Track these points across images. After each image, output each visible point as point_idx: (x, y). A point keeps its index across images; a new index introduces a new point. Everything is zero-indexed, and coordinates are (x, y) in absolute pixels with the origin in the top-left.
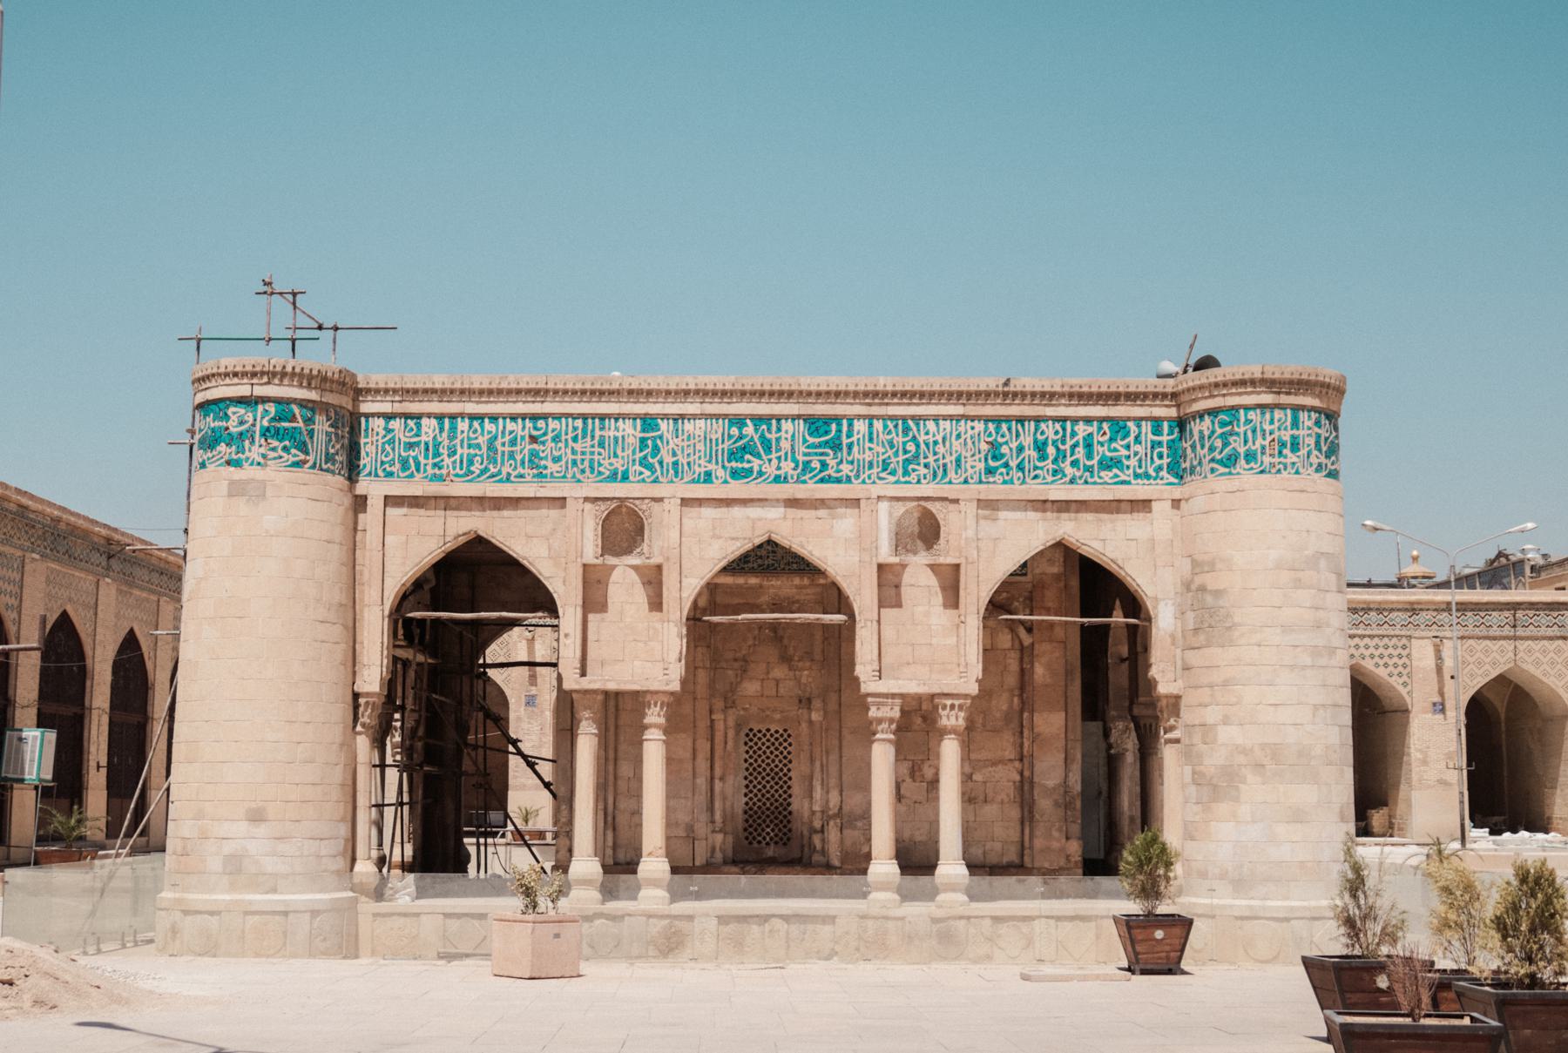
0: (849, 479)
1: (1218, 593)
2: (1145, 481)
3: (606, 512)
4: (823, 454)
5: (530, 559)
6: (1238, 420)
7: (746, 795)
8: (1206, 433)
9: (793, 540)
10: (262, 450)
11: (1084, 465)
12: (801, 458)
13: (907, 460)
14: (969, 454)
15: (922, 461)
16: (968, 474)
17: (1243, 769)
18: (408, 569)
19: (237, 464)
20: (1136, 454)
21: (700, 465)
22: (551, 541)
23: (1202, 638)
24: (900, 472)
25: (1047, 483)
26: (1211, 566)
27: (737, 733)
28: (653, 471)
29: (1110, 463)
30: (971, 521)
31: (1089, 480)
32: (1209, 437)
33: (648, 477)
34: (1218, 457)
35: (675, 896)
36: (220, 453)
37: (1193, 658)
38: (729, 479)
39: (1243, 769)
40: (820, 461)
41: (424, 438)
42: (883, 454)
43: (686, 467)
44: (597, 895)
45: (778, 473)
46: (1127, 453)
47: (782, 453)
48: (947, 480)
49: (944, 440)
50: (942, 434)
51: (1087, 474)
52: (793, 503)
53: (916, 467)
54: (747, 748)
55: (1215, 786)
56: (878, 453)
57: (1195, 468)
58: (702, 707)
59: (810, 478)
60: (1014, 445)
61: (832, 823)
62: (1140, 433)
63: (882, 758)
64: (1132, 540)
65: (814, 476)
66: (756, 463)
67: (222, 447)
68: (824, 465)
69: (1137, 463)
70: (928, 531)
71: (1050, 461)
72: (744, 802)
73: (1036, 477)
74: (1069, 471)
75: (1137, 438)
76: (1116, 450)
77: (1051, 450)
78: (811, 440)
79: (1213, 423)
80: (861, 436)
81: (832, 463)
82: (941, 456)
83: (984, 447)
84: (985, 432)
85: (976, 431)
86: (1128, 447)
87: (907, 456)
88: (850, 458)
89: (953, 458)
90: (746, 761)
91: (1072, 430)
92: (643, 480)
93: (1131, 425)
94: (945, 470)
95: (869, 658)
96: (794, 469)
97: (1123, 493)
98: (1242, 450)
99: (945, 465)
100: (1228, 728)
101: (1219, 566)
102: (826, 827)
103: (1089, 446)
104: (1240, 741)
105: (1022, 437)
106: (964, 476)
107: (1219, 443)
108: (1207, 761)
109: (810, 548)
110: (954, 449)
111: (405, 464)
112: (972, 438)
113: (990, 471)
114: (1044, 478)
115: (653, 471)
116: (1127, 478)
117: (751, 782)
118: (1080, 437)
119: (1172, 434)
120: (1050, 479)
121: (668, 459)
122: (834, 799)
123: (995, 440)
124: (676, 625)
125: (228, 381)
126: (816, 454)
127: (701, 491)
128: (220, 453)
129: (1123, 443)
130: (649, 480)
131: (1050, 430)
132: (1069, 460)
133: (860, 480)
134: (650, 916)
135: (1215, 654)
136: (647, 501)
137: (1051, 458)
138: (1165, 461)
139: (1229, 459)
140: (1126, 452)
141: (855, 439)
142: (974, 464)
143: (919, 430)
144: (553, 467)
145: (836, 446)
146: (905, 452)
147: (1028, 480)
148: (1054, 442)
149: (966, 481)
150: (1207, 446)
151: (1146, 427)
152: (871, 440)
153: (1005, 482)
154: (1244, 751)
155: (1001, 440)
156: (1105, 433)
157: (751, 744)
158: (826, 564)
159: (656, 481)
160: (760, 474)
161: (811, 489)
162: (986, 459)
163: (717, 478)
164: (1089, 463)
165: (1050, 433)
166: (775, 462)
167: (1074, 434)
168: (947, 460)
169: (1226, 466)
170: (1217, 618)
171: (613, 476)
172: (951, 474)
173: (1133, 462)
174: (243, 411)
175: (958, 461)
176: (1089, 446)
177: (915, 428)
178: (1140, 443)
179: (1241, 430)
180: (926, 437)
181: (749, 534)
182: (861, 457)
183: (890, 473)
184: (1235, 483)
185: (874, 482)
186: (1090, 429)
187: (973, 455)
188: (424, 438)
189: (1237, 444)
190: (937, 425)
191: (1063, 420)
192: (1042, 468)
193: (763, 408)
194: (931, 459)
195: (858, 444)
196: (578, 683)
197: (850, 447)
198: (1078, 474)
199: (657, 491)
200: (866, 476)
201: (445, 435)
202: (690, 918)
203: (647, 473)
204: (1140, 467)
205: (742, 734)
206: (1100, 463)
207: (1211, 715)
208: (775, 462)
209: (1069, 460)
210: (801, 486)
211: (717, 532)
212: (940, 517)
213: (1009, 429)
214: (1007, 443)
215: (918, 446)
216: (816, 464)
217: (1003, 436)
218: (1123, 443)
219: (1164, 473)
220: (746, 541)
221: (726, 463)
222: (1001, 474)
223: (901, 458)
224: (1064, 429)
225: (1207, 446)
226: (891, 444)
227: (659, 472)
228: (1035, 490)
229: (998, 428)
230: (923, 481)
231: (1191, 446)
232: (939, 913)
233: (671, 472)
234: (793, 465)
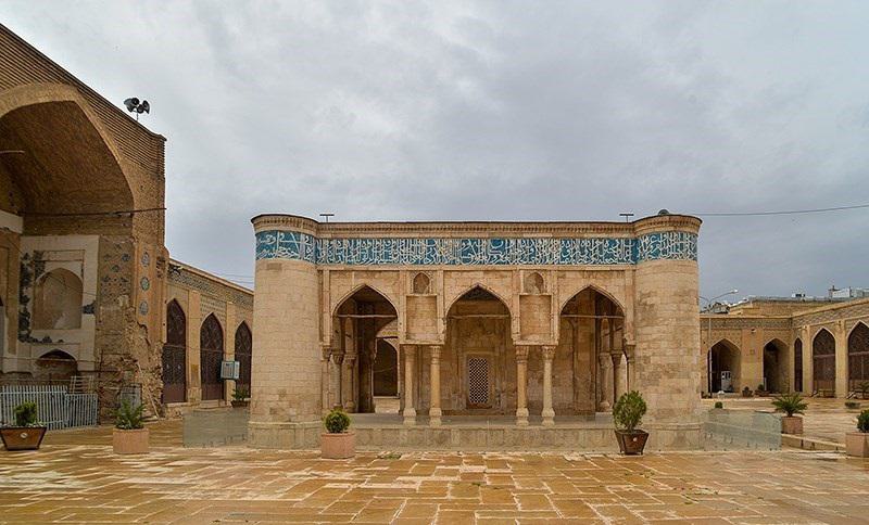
19: (271, 257)
30: (556, 279)
35: (444, 421)
44: (414, 422)
52: (486, 271)
58: (454, 351)
63: (521, 369)
68: (499, 258)
70: (539, 281)
74: (593, 259)
77: (586, 251)
97: (614, 267)
103: (601, 250)
113: (563, 259)
154: (660, 366)
171: (417, 263)
184: (658, 263)
193: (475, 235)
228: (580, 266)
232: (542, 428)
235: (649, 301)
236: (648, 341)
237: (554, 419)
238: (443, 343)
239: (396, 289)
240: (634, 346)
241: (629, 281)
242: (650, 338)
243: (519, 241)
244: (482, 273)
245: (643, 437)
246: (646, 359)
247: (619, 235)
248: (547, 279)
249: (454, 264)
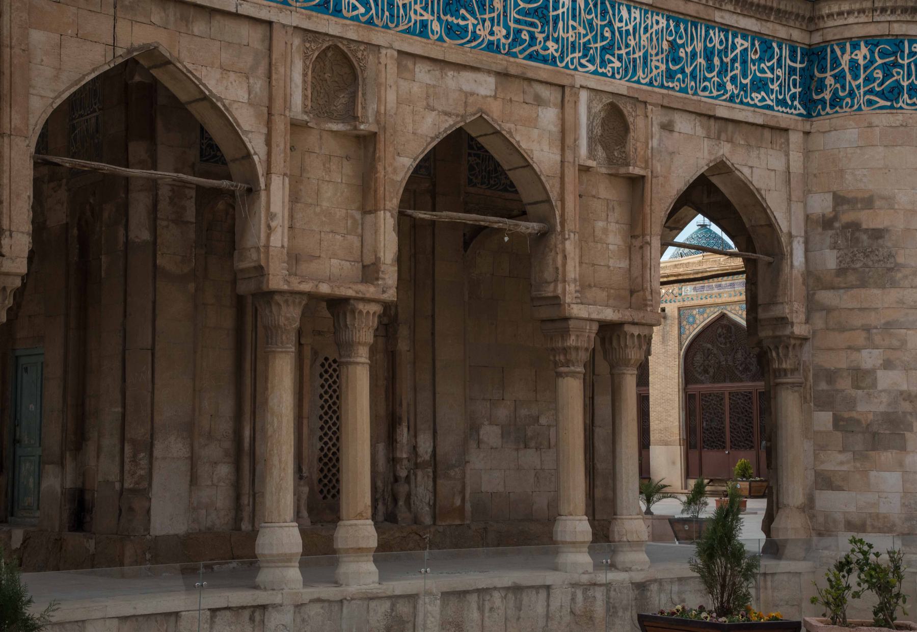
0: (554, 61)
1: (878, 234)
2: (784, 109)
3: (316, 54)
4: (532, 25)
5: (227, 102)
6: (903, 52)
7: (321, 439)
8: (862, 62)
9: (503, 125)
11: (741, 82)
12: (512, 25)
13: (603, 48)
14: (654, 52)
15: (617, 52)
16: (653, 75)
17: (909, 417)
18: (63, 87)
20: (778, 78)
21: (415, 12)
22: (251, 81)
23: (852, 278)
24: (598, 61)
25: (712, 97)
26: (868, 202)
27: (314, 361)
29: (760, 85)
30: (656, 129)
31: (745, 101)
32: (866, 68)
33: (363, 15)
34: (878, 89)
37: (826, 297)
38: (446, 39)
39: (909, 417)
40: (529, 32)
42: (585, 36)
43: (401, 11)
45: (491, 38)
46: (771, 76)
47: (495, 15)
48: (636, 78)
49: (634, 29)
50: (633, 24)
51: (742, 93)
53: (611, 58)
54: (322, 381)
55: (874, 435)
56: (579, 33)
57: (842, 99)
59: (522, 51)
60: (689, 50)
61: (420, 473)
62: (781, 56)
64: (772, 170)
65: (524, 50)
66: (471, 21)
68: (533, 37)
69: (778, 88)
71: (715, 73)
72: (319, 447)
73: (705, 89)
74: (729, 86)
75: (779, 60)
76: (763, 71)
77: (716, 61)
78: (522, 5)
79: (872, 52)
80: (565, 10)
81: (540, 37)
82: (631, 49)
83: (665, 45)
84: (667, 29)
85: (660, 26)
86: (772, 69)
87: (604, 43)
88: (556, 35)
89: (641, 54)
90: (321, 396)
91: (733, 42)
92: (355, 19)
93: (774, 45)
94: (635, 66)
95: (573, 277)
96: (507, 37)
98: (905, 84)
99: (635, 60)
100: (891, 373)
101: (878, 203)
102: (413, 477)
103: (744, 62)
104: (904, 387)
105: (695, 42)
106: (649, 76)
107: (879, 74)
108: (862, 407)
109: (518, 138)
110: (642, 43)
112: (657, 33)
113: (670, 75)
114: (711, 92)
115: (369, 9)
116: (772, 104)
117: (326, 422)
118: (738, 51)
119: (804, 63)
120: (715, 93)
122: (425, 446)
123: (675, 40)
124: (392, 216)
126: (526, 23)
127: (415, 45)
129: (769, 64)
130: (363, 19)
131: (716, 37)
132: (730, 74)
133: (564, 64)
134: (371, 599)
135: (874, 296)
136: (362, 48)
137: (717, 70)
138: (798, 90)
139: (890, 92)
140: (769, 75)
141: (560, 11)
142: (657, 64)
143: (614, 15)
145: (544, 19)
146: (603, 38)
147: (699, 91)
148: (720, 52)
149: (651, 84)
150: (862, 76)
151: (786, 52)
152: (574, 17)
153: (682, 90)
155: (680, 42)
156: (756, 52)
157: (326, 376)
158: (532, 159)
159: (370, 22)
160: (475, 37)
161: (519, 63)
162: (667, 61)
163: (432, 31)
164: (744, 82)
165: (716, 41)
166: (488, 23)
167: (734, 47)
168: (636, 56)
169: (887, 99)
170: (876, 258)
172: (640, 73)
173: (775, 87)
175: (645, 58)
176: (744, 62)
177: (611, 12)
178: (781, 67)
179: (906, 62)
180: (620, 25)
181: (461, 111)
182: (565, 36)
183: (588, 61)
184: (898, 119)
185: (576, 69)
186: (746, 44)
187: (657, 54)
190: (629, 13)
191: (725, 28)
192: (709, 80)
194: (623, 52)
195: (563, 20)
196: (288, 282)
197: (556, 23)
198: (736, 92)
199: (378, 37)
200: (569, 58)
202: (412, 598)
203: (362, 10)
204: (781, 94)
205: (318, 363)
206: (752, 82)
207: (869, 359)
208: (488, 23)
209: (730, 74)
210: (512, 59)
211: (431, 101)
212: (630, 120)
213: (686, 30)
214: (683, 46)
215: (613, 33)
216: (525, 36)
217: (681, 38)
218: (769, 64)
219: (796, 103)
220: (459, 119)
221: (442, 16)
222: (679, 80)
223: (599, 45)
224: (727, 40)
225: (862, 76)
226: (590, 23)
227: (373, 11)
229: (677, 26)
230: (616, 75)
231: (835, 77)
232: (639, 577)
233: (387, 13)
234: (504, 32)
235: (868, 219)
236: (867, 329)
237: (592, 551)
238: (391, 295)
239: (259, 85)
240: (805, 339)
241: (796, 160)
242: (872, 319)
244: (491, 80)
245: (859, 597)
246: (861, 376)
247: (782, 32)
248: (637, 122)
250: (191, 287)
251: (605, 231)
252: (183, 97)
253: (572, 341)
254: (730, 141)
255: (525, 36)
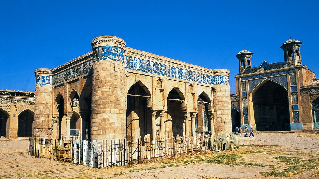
8: (219, 79)
10: (119, 58)
19: (115, 60)
28: (162, 73)
36: (110, 57)
41: (132, 61)
67: (111, 56)
74: (204, 81)
98: (224, 81)
107: (221, 80)
111: (129, 65)
121: (165, 72)
125: (112, 42)
127: (169, 78)
128: (110, 57)
144: (150, 71)
171: (158, 74)
174: (115, 49)
188: (132, 61)
189: (224, 80)
191: (203, 74)
201: (135, 61)
216: (181, 76)
243: (187, 71)
249: (169, 76)
250: (139, 109)
251: (190, 100)
252: (142, 86)
253: (187, 115)
254: (205, 88)
255: (181, 76)
